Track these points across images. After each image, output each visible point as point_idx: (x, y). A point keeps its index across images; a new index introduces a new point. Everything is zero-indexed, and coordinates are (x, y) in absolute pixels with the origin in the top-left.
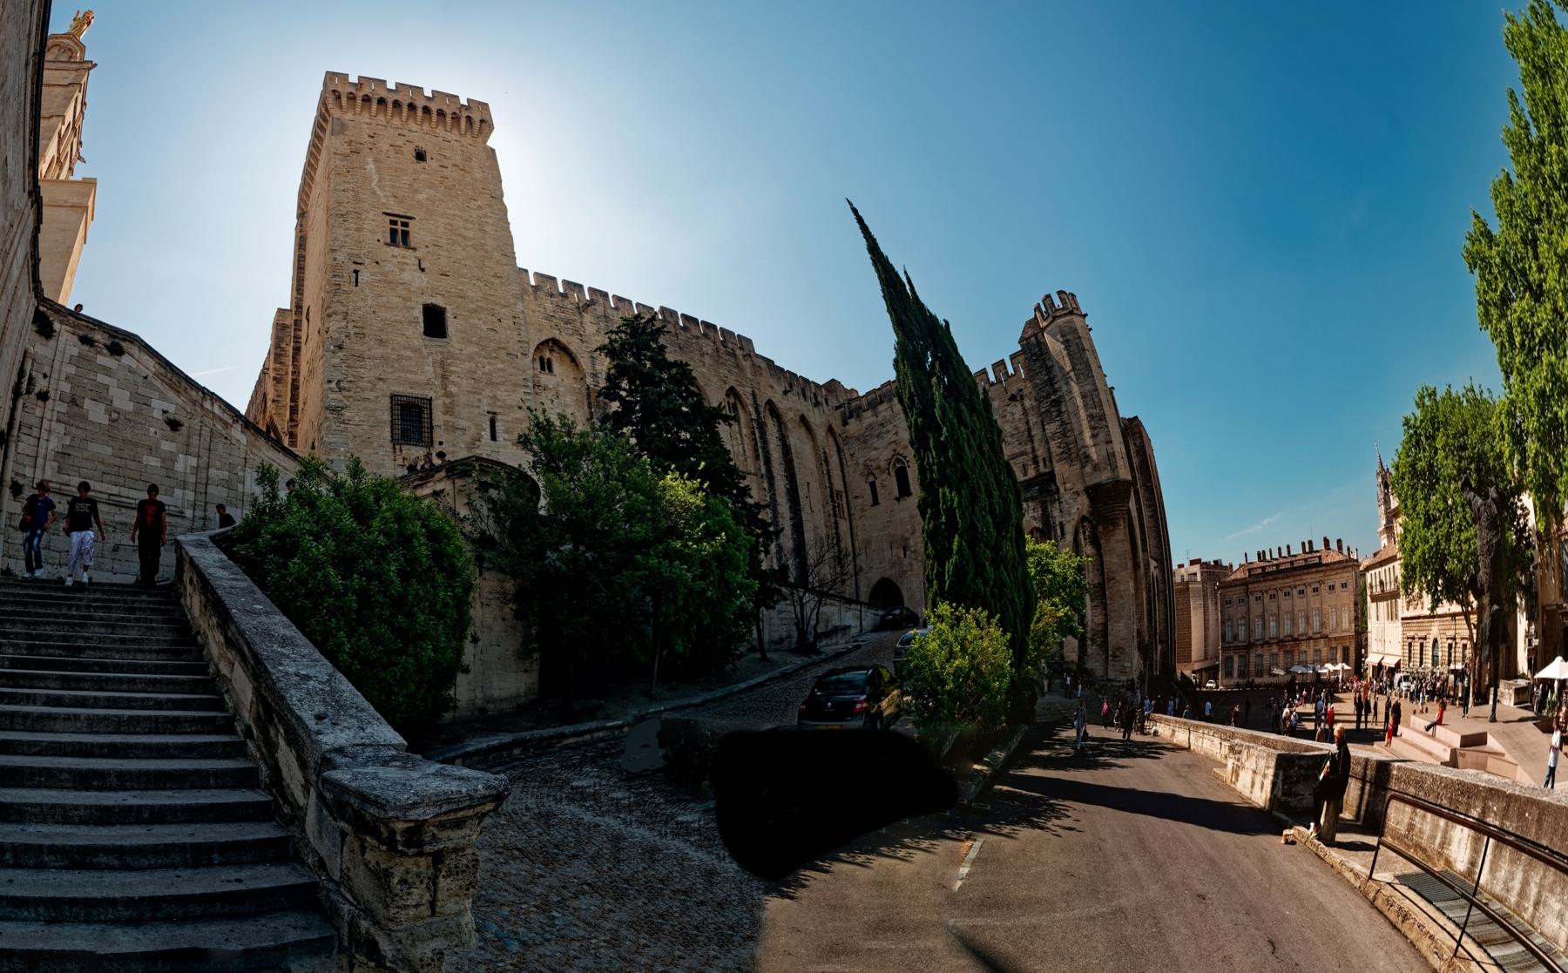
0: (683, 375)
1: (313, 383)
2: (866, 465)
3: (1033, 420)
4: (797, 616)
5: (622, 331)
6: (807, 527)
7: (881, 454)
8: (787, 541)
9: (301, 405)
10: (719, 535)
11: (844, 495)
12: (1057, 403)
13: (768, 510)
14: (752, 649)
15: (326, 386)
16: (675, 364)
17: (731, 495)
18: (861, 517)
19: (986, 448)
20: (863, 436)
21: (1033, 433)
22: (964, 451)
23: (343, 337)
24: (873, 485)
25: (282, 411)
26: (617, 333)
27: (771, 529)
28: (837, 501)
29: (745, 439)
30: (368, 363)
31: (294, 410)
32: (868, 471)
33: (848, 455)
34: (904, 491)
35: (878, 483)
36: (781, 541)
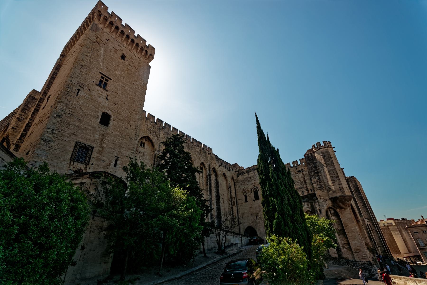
0: (188, 156)
1: (39, 127)
2: (243, 190)
3: (306, 178)
4: (217, 239)
5: (171, 139)
6: (222, 208)
7: (249, 186)
8: (214, 213)
9: (28, 134)
10: (190, 209)
11: (235, 198)
12: (318, 173)
13: (209, 202)
14: (201, 253)
15: (46, 130)
16: (186, 153)
17: (196, 196)
18: (241, 206)
19: (287, 186)
20: (243, 180)
21: (306, 182)
22: (279, 186)
23: (62, 113)
24: (246, 196)
25: (16, 134)
26: (169, 139)
27: (209, 208)
28: (233, 200)
29: (204, 179)
30: (71, 127)
31: (23, 135)
32: (244, 191)
33: (237, 186)
34: (257, 198)
35: (247, 195)
36: (212, 212)
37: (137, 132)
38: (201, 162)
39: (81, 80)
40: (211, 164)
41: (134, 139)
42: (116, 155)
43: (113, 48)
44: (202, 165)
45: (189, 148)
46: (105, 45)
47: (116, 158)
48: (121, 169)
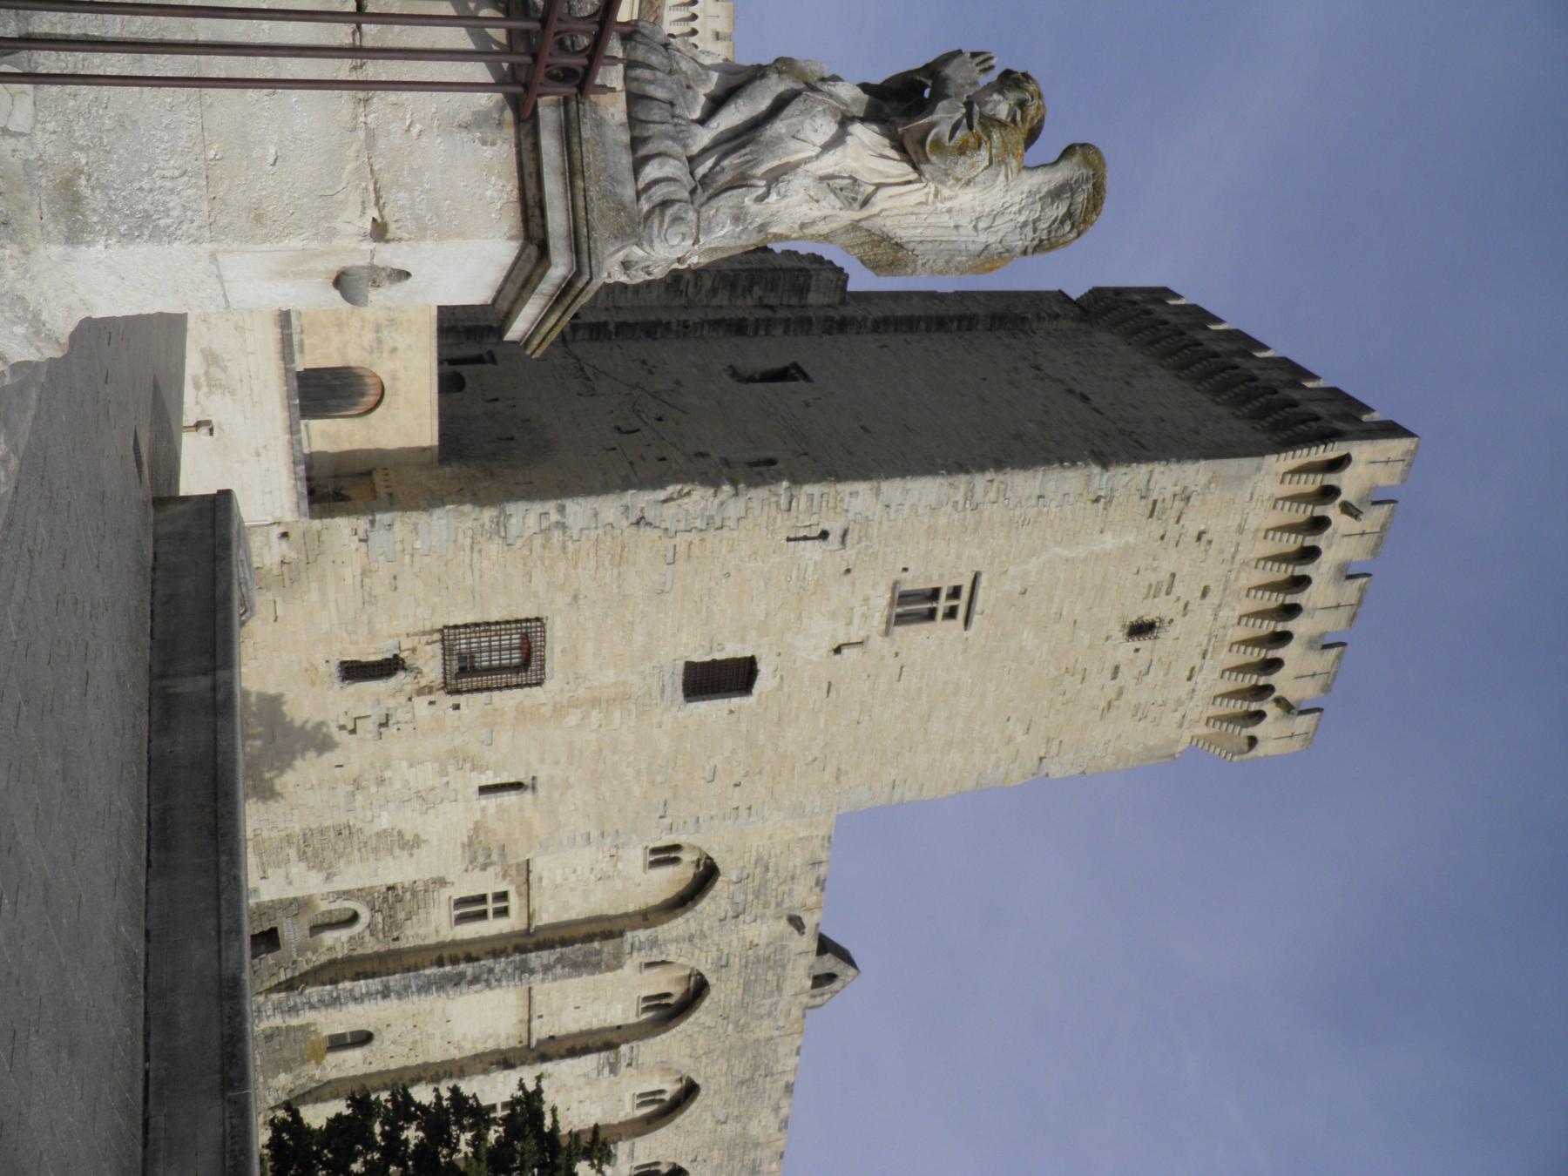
37: (716, 823)
39: (885, 522)
41: (667, 821)
43: (1173, 575)
46: (1162, 538)
47: (527, 781)
48: (478, 816)
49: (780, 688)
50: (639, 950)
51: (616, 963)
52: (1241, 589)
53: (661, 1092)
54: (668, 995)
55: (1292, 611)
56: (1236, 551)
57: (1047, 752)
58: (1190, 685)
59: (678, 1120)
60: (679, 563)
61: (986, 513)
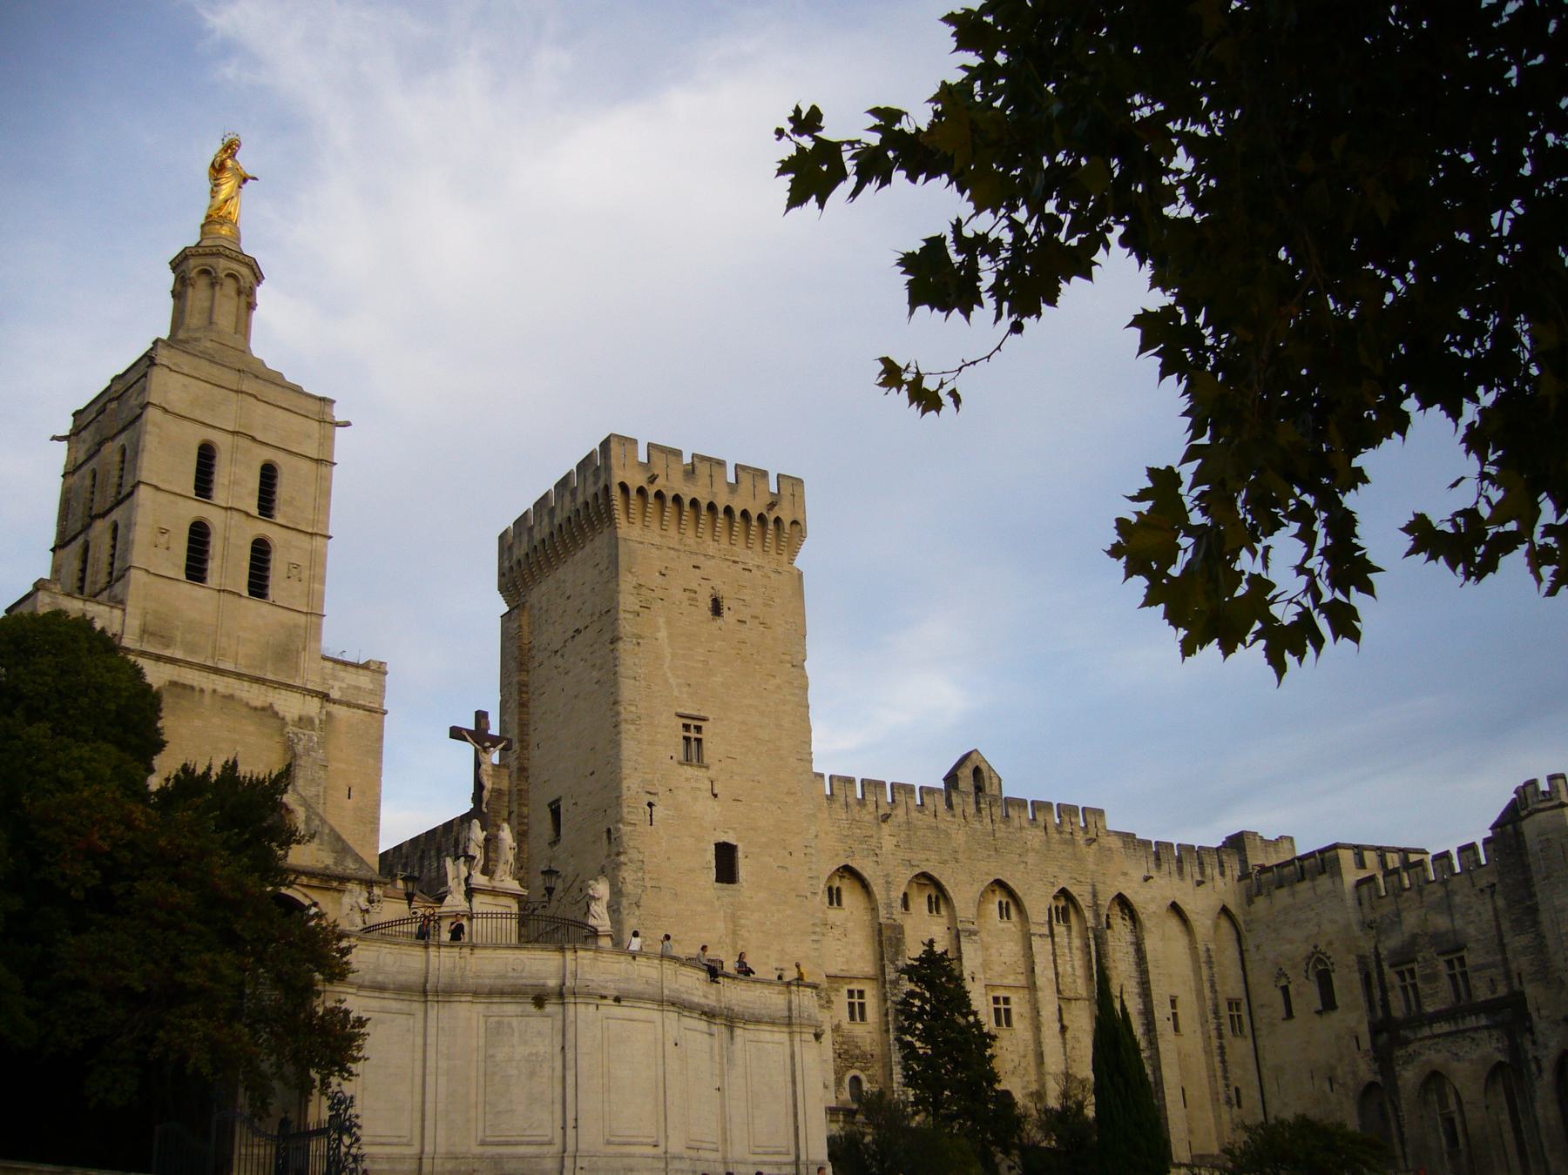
3: (1506, 925)
11: (1245, 1001)
12: (1534, 910)
21: (1505, 941)
24: (1285, 990)
34: (1328, 1003)
35: (1291, 988)
38: (1056, 890)
40: (1104, 883)
41: (809, 895)
42: (775, 965)
44: (1062, 899)
45: (996, 850)
49: (734, 829)
50: (892, 914)
51: (899, 929)
52: (698, 543)
53: (1000, 903)
54: (930, 897)
55: (712, 507)
56: (673, 549)
57: (789, 662)
58: (754, 570)
59: (1020, 894)
60: (661, 884)
61: (643, 711)
